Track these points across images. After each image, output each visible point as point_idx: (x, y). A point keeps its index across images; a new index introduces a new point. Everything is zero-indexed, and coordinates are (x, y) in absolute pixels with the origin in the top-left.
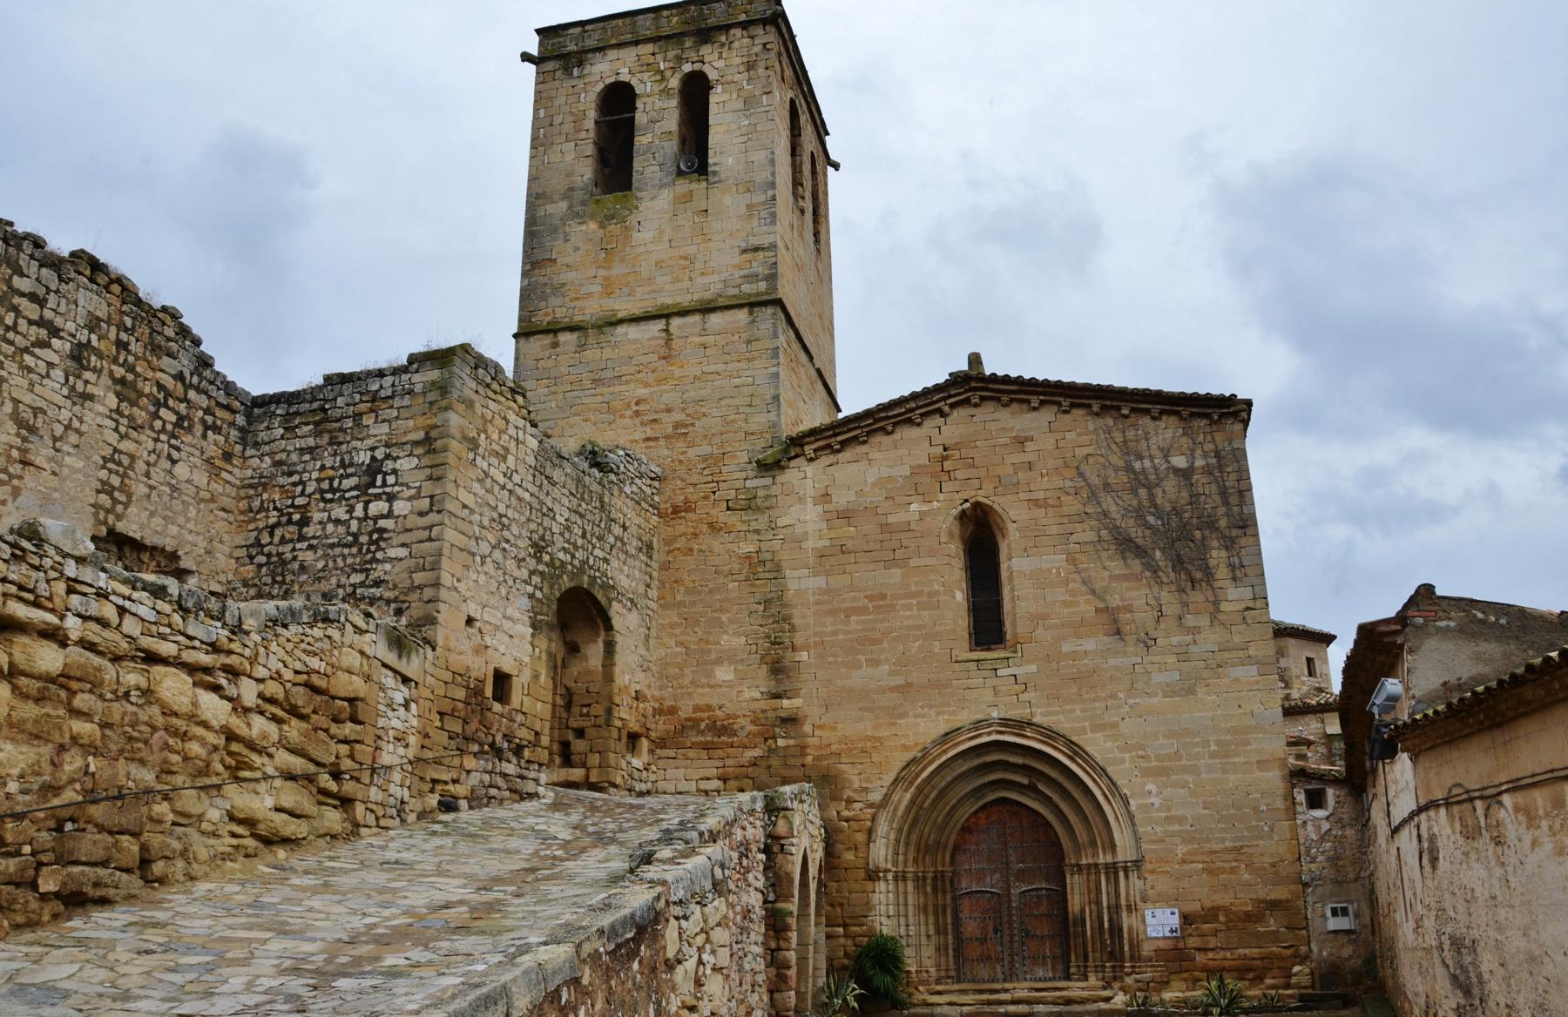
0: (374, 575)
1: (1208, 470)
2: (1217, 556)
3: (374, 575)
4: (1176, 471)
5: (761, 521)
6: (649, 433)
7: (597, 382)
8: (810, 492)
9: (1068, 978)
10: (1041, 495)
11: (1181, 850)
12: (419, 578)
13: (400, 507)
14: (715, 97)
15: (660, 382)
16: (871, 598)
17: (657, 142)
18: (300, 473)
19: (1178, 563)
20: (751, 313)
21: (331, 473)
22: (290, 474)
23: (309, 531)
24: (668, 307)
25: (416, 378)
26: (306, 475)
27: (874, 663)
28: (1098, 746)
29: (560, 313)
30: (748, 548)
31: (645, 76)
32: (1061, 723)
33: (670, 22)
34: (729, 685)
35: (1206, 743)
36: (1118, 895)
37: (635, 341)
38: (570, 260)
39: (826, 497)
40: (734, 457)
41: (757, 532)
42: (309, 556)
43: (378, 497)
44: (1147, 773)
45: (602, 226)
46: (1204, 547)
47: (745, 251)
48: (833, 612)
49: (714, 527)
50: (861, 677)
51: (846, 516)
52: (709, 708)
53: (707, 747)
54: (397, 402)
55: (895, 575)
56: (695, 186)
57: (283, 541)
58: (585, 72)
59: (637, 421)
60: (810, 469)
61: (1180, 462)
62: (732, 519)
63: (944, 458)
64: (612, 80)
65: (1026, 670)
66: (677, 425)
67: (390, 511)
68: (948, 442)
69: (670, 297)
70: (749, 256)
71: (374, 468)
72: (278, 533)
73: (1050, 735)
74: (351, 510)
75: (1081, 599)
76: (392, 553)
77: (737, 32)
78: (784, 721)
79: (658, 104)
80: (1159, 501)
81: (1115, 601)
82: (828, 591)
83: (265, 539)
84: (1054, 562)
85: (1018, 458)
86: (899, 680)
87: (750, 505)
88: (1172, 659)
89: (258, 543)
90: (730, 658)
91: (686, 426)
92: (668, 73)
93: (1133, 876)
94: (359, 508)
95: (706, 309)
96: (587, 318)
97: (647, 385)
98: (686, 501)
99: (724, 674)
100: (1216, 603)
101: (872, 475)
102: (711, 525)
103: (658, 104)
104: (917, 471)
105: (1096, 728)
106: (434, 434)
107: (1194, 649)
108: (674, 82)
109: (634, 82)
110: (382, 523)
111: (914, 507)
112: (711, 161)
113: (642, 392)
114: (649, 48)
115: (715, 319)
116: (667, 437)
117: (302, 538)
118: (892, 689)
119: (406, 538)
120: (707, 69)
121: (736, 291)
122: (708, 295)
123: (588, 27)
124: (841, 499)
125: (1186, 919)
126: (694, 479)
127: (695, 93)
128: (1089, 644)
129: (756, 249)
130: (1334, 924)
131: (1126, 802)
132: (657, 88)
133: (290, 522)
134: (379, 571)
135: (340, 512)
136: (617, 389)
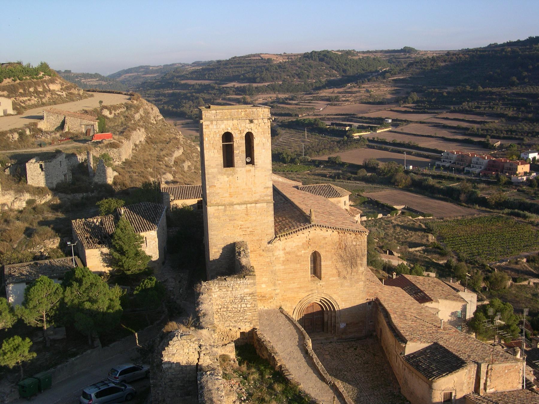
0: (245, 318)
2: (359, 262)
3: (245, 318)
5: (270, 254)
6: (244, 234)
8: (281, 248)
9: (323, 331)
10: (328, 249)
12: (254, 318)
13: (248, 306)
14: (256, 141)
15: (246, 221)
16: (293, 270)
17: (240, 153)
18: (225, 298)
20: (267, 205)
21: (232, 299)
24: (246, 201)
25: (248, 281)
26: (226, 299)
27: (294, 283)
28: (335, 297)
29: (218, 201)
30: (268, 260)
33: (241, 114)
34: (264, 288)
35: (353, 296)
36: (336, 320)
37: (239, 210)
38: (220, 186)
39: (284, 249)
40: (264, 239)
41: (270, 256)
42: (230, 314)
43: (243, 304)
44: (343, 301)
45: (228, 177)
47: (265, 188)
48: (286, 273)
50: (292, 286)
51: (289, 253)
52: (261, 292)
53: (261, 300)
54: (245, 286)
55: (298, 266)
56: (251, 168)
58: (218, 127)
59: (241, 230)
61: (354, 243)
63: (309, 241)
64: (226, 131)
65: (322, 283)
66: (250, 232)
67: (246, 307)
68: (310, 238)
70: (266, 189)
71: (242, 299)
72: (222, 310)
73: (327, 294)
74: (238, 306)
75: (334, 270)
78: (276, 294)
79: (240, 141)
81: (340, 270)
82: (285, 269)
83: (219, 310)
84: (329, 263)
85: (323, 242)
86: (299, 286)
87: (269, 250)
88: (349, 281)
90: (264, 282)
91: (253, 232)
92: (242, 132)
93: (339, 319)
94: (240, 306)
95: (256, 202)
96: (226, 203)
97: (242, 221)
98: (254, 249)
99: (264, 286)
100: (358, 271)
101: (294, 245)
102: (260, 255)
103: (240, 141)
104: (303, 244)
105: (334, 294)
106: (253, 293)
107: (353, 279)
108: (244, 135)
110: (245, 308)
111: (303, 252)
112: (255, 161)
113: (241, 222)
114: (235, 122)
115: (258, 205)
116: (249, 234)
117: (227, 311)
118: (298, 288)
119: (251, 311)
120: (253, 132)
121: (263, 199)
122: (256, 199)
123: (218, 111)
124: (288, 250)
125: (347, 324)
126: (255, 244)
127: (249, 138)
128: (335, 279)
129: (268, 188)
131: (338, 306)
132: (240, 136)
133: (224, 308)
134: (246, 317)
135: (236, 306)
136: (235, 222)
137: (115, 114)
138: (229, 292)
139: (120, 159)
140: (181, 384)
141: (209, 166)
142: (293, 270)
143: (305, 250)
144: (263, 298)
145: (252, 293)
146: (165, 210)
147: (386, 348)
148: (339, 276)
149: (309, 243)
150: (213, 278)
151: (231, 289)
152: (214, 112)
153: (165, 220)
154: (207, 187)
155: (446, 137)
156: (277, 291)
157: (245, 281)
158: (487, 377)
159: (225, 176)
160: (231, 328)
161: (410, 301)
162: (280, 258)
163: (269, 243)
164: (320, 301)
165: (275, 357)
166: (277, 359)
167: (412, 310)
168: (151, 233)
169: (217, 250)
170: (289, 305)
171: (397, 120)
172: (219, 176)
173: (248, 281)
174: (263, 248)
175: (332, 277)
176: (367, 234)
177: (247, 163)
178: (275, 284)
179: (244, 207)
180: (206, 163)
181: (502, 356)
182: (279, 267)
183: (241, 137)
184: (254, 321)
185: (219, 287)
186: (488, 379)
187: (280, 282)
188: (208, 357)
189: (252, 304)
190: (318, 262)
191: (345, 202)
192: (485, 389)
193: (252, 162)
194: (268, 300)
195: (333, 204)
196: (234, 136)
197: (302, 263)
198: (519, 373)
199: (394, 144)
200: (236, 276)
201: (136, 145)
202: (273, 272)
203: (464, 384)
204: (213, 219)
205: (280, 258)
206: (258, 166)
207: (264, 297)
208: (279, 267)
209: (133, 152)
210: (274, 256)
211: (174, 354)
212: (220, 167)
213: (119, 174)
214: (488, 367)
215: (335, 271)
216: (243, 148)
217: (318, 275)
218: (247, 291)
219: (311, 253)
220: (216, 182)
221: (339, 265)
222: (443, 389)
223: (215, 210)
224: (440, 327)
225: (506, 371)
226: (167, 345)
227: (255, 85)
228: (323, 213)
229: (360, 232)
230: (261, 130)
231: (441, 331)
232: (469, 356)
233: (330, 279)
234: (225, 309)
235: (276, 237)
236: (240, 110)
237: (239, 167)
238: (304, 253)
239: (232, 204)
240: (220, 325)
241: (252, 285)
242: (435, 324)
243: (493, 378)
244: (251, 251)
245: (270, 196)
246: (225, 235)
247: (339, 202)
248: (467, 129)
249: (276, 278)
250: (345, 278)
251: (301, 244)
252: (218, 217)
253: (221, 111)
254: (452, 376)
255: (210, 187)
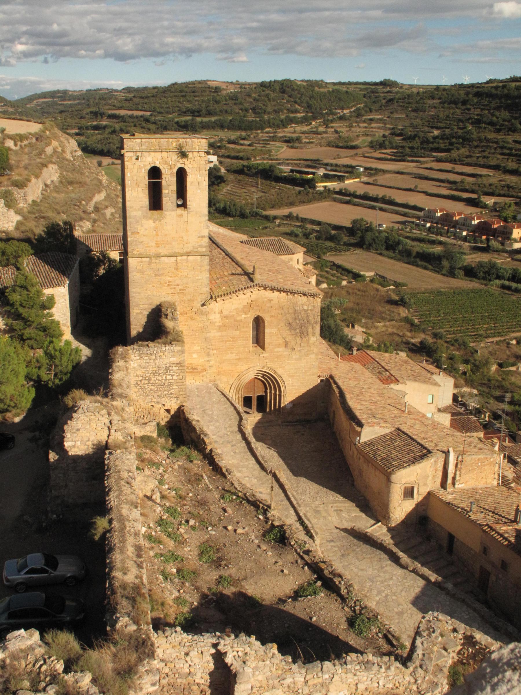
1: (311, 310)
2: (310, 330)
4: (304, 310)
5: (204, 318)
6: (172, 291)
7: (156, 275)
10: (273, 314)
11: (294, 391)
12: (181, 393)
13: (175, 378)
14: (190, 179)
15: (175, 277)
16: (232, 338)
19: (301, 332)
22: (144, 368)
23: (151, 382)
24: (175, 253)
25: (175, 348)
27: (232, 353)
28: (280, 371)
29: (142, 251)
31: (165, 166)
32: (273, 366)
37: (167, 263)
39: (221, 312)
42: (153, 387)
44: (290, 377)
45: (154, 222)
46: (307, 328)
47: (199, 237)
48: (222, 341)
49: (192, 319)
51: (226, 317)
52: (191, 364)
53: (191, 373)
55: (237, 333)
57: (144, 384)
58: (144, 160)
60: (217, 304)
61: (305, 308)
62: (195, 316)
64: (153, 165)
65: (266, 355)
66: (180, 290)
67: (172, 379)
69: (177, 249)
71: (167, 369)
72: (143, 382)
73: (271, 369)
76: (174, 387)
77: (195, 154)
80: (300, 316)
81: (287, 339)
83: (139, 383)
84: (274, 330)
85: (268, 305)
86: (238, 357)
87: (202, 313)
89: (137, 384)
92: (173, 166)
94: (164, 378)
95: (188, 254)
99: (195, 356)
101: (233, 307)
104: (244, 306)
105: (280, 367)
108: (175, 171)
109: (161, 168)
111: (243, 316)
112: (188, 203)
113: (169, 278)
114: (165, 154)
115: (190, 258)
117: (149, 383)
120: (186, 168)
121: (196, 250)
122: (189, 250)
123: (143, 140)
124: (225, 313)
125: (294, 405)
128: (280, 349)
129: (202, 237)
130: (322, 405)
131: (284, 382)
132: (170, 172)
134: (171, 391)
135: (160, 378)
137: (21, 146)
138: (152, 361)
139: (25, 200)
140: (87, 466)
141: (131, 207)
142: (232, 338)
143: (246, 314)
144: (194, 370)
145: (180, 363)
146: (77, 262)
147: (339, 434)
148: (286, 346)
149: (251, 306)
150: (133, 343)
151: (154, 357)
152: (139, 140)
153: (78, 274)
154: (129, 233)
155: (430, 191)
156: (211, 363)
157: (172, 348)
158: (456, 471)
159: (151, 221)
160: (153, 404)
161: (370, 380)
162: (216, 322)
163: (203, 305)
164: (263, 377)
165: (205, 439)
166: (207, 441)
167: (372, 391)
168: (60, 290)
169: (138, 311)
170: (225, 379)
171: (370, 169)
172: (144, 221)
173: (175, 348)
174: (195, 310)
175: (278, 347)
176: (321, 297)
177: (178, 206)
178: (208, 355)
179: (173, 259)
180: (128, 204)
181: (475, 446)
182: (214, 334)
183: (172, 174)
184: (181, 397)
185: (140, 355)
186: (458, 473)
187: (215, 352)
188: (119, 434)
189: (179, 376)
190: (262, 329)
191: (298, 260)
192: (454, 484)
193: (184, 205)
194: (200, 372)
195: (283, 261)
196: (163, 171)
197: (243, 330)
198: (494, 466)
199: (365, 197)
200: (160, 341)
201: (46, 185)
202: (208, 340)
203: (428, 477)
204: (135, 273)
205: (216, 322)
206: (191, 210)
207: (195, 369)
208: (214, 334)
209: (42, 194)
210: (208, 319)
211: (78, 430)
212: (145, 209)
213: (23, 217)
214: (457, 458)
215: (281, 341)
216: (174, 187)
217: (261, 344)
218: (173, 360)
219: (253, 318)
220: (139, 227)
221: (287, 334)
222: (403, 482)
223: (138, 262)
224: (404, 411)
225: (479, 464)
226: (71, 418)
227: (199, 119)
228: (270, 270)
229: (313, 296)
230: (196, 166)
231: (405, 415)
232: (436, 445)
233: (276, 350)
234: (146, 382)
235: (212, 298)
236: (171, 140)
237: (167, 210)
238: (245, 318)
239: (158, 256)
240: (140, 401)
241: (180, 353)
242: (399, 407)
243: (463, 471)
244: (181, 314)
245: (205, 247)
246: (149, 293)
247: (291, 260)
248: (454, 183)
249: (211, 347)
250: (293, 349)
251: (241, 306)
252: (142, 272)
253: (148, 140)
254: (415, 467)
255: (132, 233)
